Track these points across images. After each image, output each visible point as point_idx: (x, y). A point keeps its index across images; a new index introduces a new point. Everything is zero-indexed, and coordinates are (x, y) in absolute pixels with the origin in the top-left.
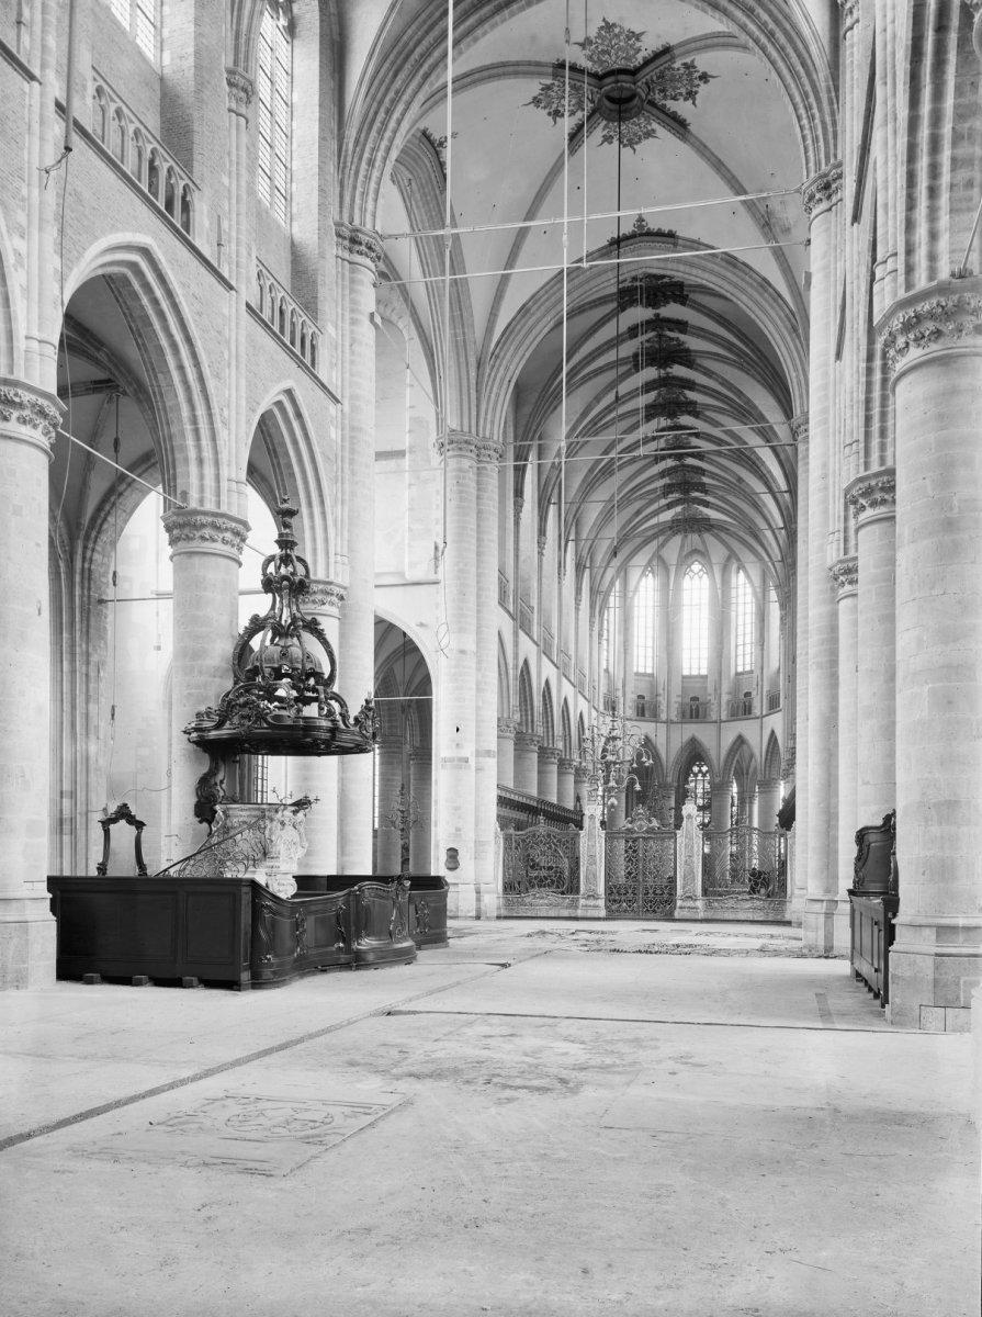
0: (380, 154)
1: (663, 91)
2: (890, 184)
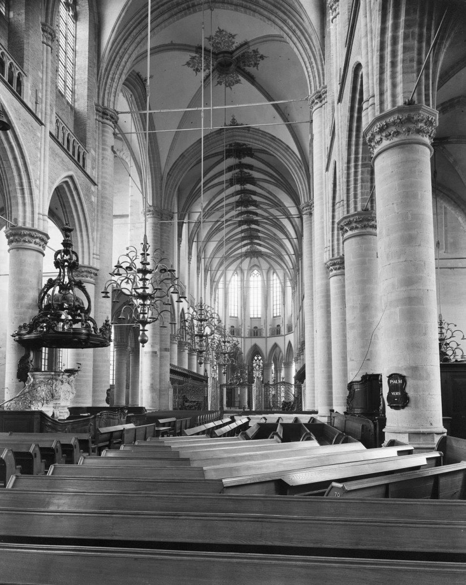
0: (117, 76)
1: (244, 62)
2: (370, 64)
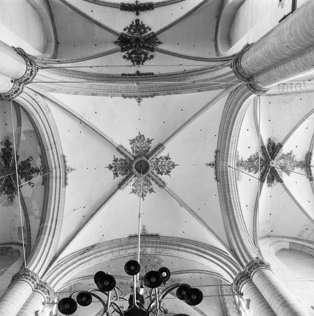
1: (126, 164)
